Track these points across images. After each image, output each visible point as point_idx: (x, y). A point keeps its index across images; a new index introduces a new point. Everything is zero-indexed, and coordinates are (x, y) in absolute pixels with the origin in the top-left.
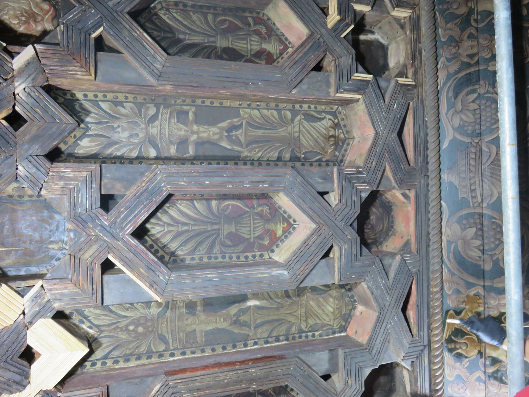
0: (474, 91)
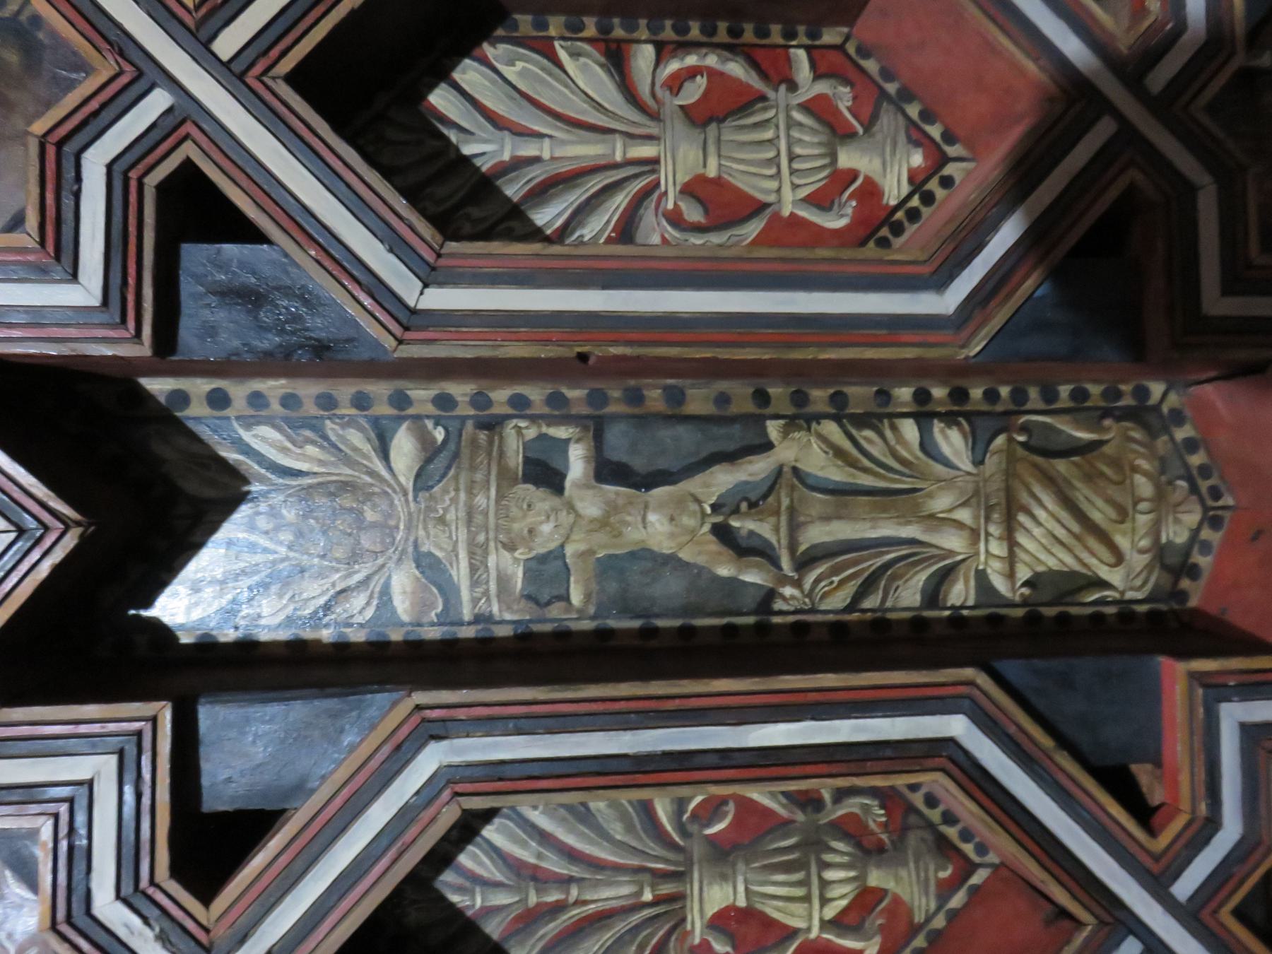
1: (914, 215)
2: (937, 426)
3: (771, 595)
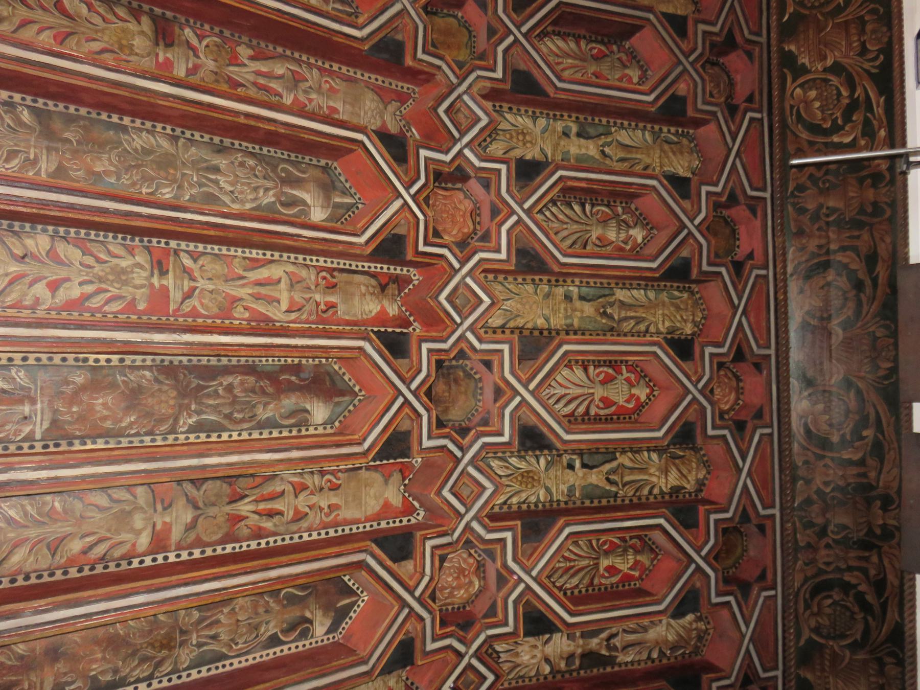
0: (830, 597)
1: (647, 404)
3: (617, 493)
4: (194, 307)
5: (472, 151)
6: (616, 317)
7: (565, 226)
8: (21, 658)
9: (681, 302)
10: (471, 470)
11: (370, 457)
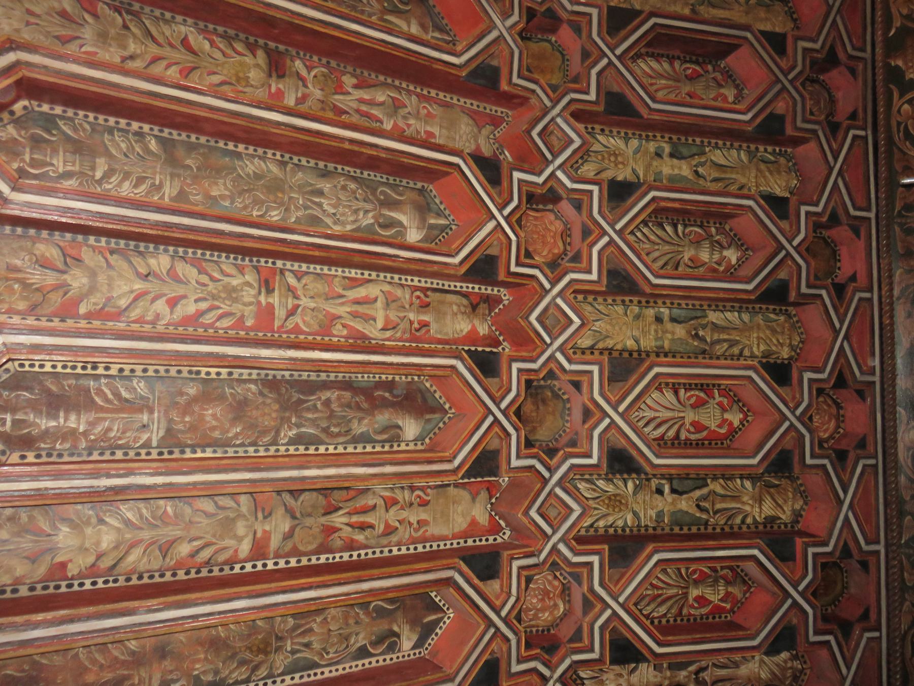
2: (745, 481)
4: (297, 324)
5: (564, 172)
6: (708, 340)
7: (657, 247)
8: (133, 653)
9: (778, 325)
10: (558, 491)
11: (460, 475)
